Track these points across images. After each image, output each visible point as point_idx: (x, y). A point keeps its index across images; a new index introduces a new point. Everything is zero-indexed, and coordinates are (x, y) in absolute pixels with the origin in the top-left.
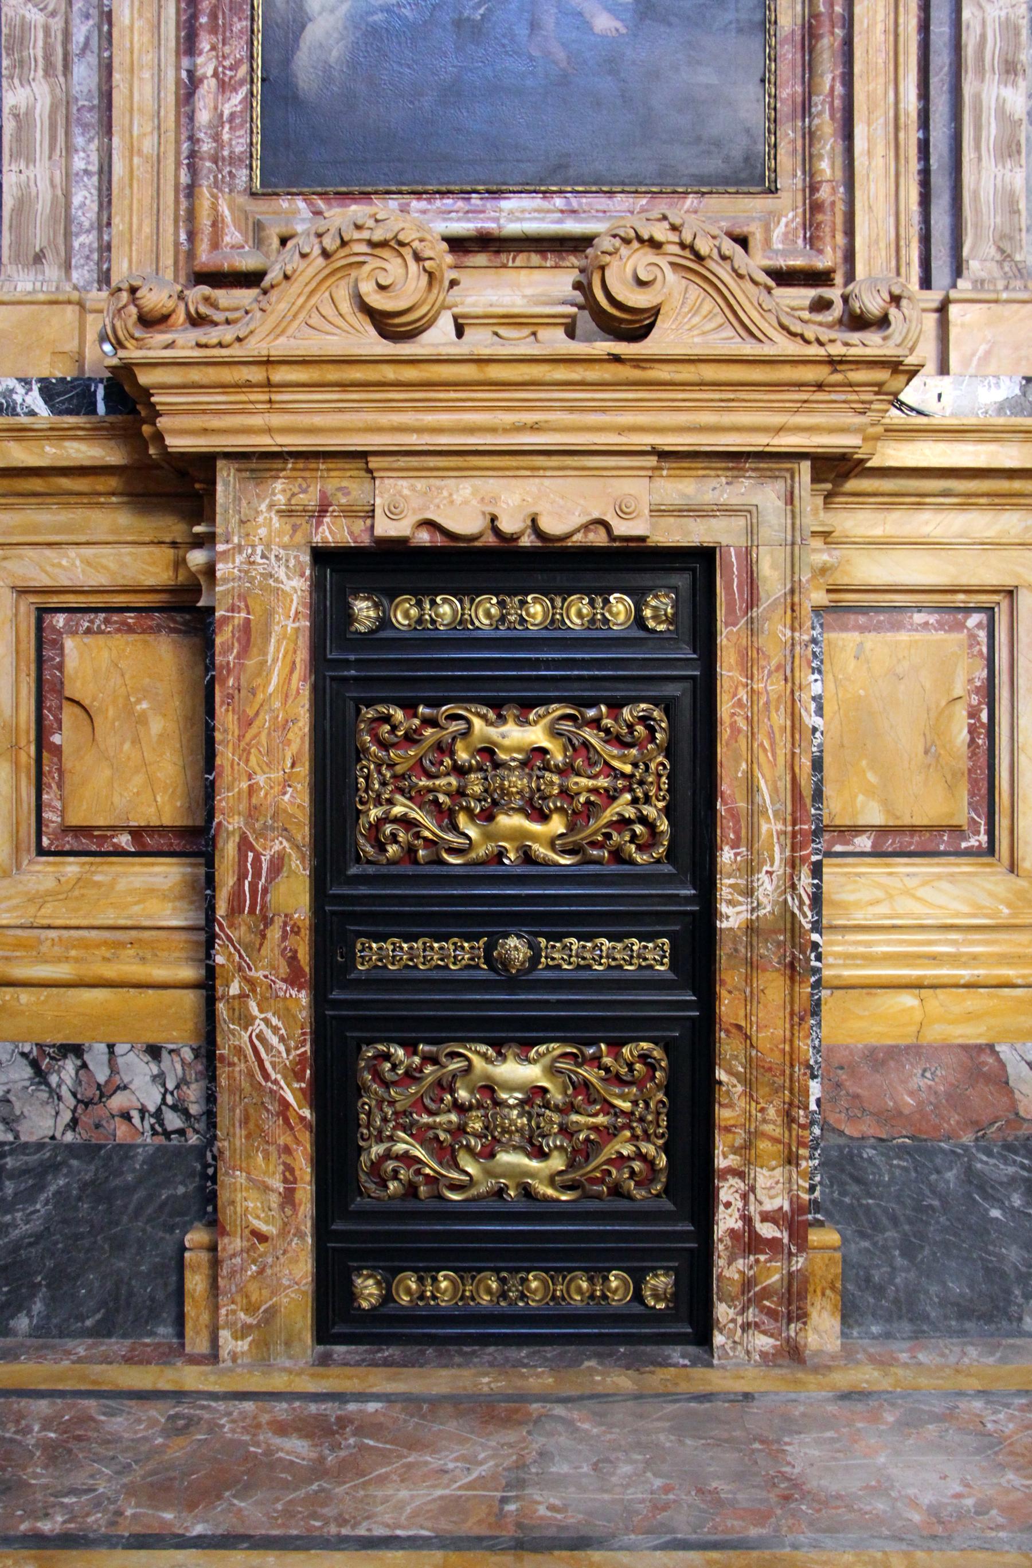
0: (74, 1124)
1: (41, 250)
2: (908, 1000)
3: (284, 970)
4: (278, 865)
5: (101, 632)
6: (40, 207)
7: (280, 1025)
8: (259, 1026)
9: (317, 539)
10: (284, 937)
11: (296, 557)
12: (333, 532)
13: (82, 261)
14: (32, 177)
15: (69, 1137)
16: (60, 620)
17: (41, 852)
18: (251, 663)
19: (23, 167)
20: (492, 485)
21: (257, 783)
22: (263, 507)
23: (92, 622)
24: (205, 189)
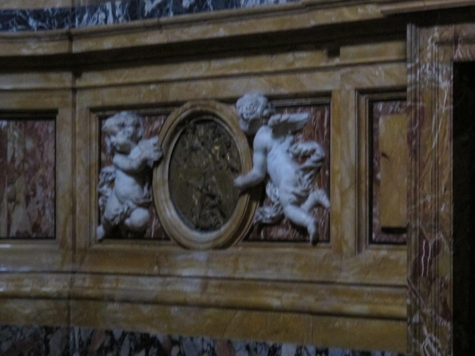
3: (441, 309)
4: (437, 248)
5: (397, 113)
7: (438, 341)
8: (427, 341)
9: (455, 57)
10: (441, 290)
11: (446, 69)
12: (461, 53)
16: (380, 106)
17: (372, 241)
18: (425, 131)
21: (427, 201)
22: (429, 40)
23: (394, 107)
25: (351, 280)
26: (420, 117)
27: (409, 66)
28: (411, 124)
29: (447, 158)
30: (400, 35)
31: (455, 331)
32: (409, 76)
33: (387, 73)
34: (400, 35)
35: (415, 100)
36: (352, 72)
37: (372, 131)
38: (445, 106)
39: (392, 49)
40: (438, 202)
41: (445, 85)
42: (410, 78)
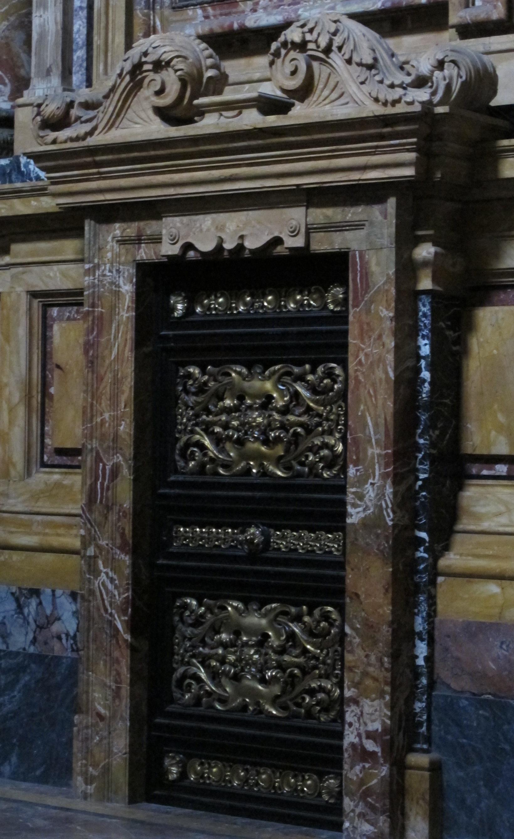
0: (34, 641)
1: (50, 67)
2: (493, 588)
3: (118, 541)
4: (115, 472)
5: (75, 319)
6: (49, 38)
7: (115, 577)
8: (103, 577)
9: (138, 258)
10: (119, 520)
11: (128, 270)
12: (145, 253)
13: (78, 68)
14: (46, 18)
15: (32, 650)
16: (55, 311)
17: (44, 465)
18: (103, 340)
19: (42, 13)
20: (222, 217)
21: (105, 418)
22: (110, 239)
23: (70, 312)
24: (138, 12)
25: (20, 508)
26: (99, 324)
27: (87, 266)
28: (89, 331)
29: (128, 371)
30: (77, 232)
31: (134, 565)
32: (87, 278)
33: (64, 275)
34: (78, 232)
35: (93, 306)
36: (24, 273)
37: (45, 339)
38: (126, 313)
39: (68, 247)
40: (116, 420)
41: (127, 289)
42: (88, 280)
